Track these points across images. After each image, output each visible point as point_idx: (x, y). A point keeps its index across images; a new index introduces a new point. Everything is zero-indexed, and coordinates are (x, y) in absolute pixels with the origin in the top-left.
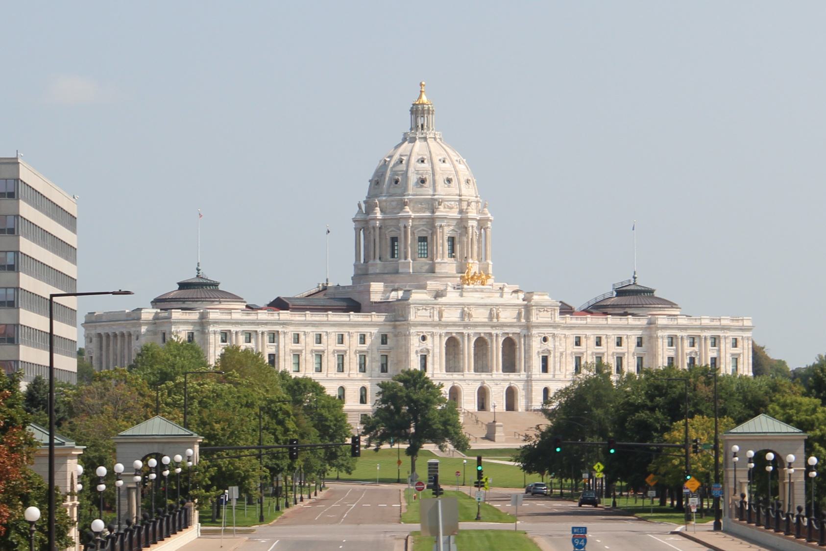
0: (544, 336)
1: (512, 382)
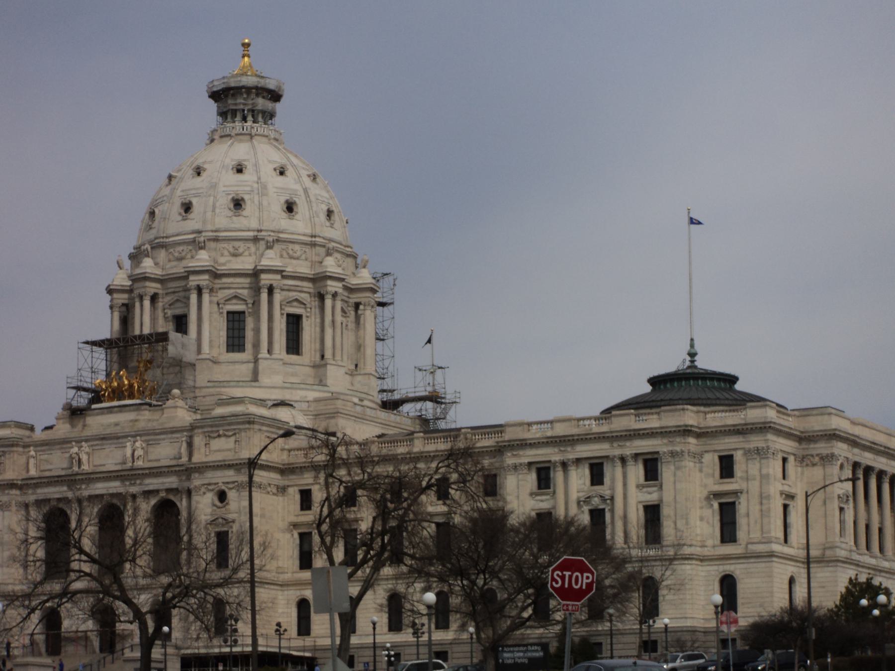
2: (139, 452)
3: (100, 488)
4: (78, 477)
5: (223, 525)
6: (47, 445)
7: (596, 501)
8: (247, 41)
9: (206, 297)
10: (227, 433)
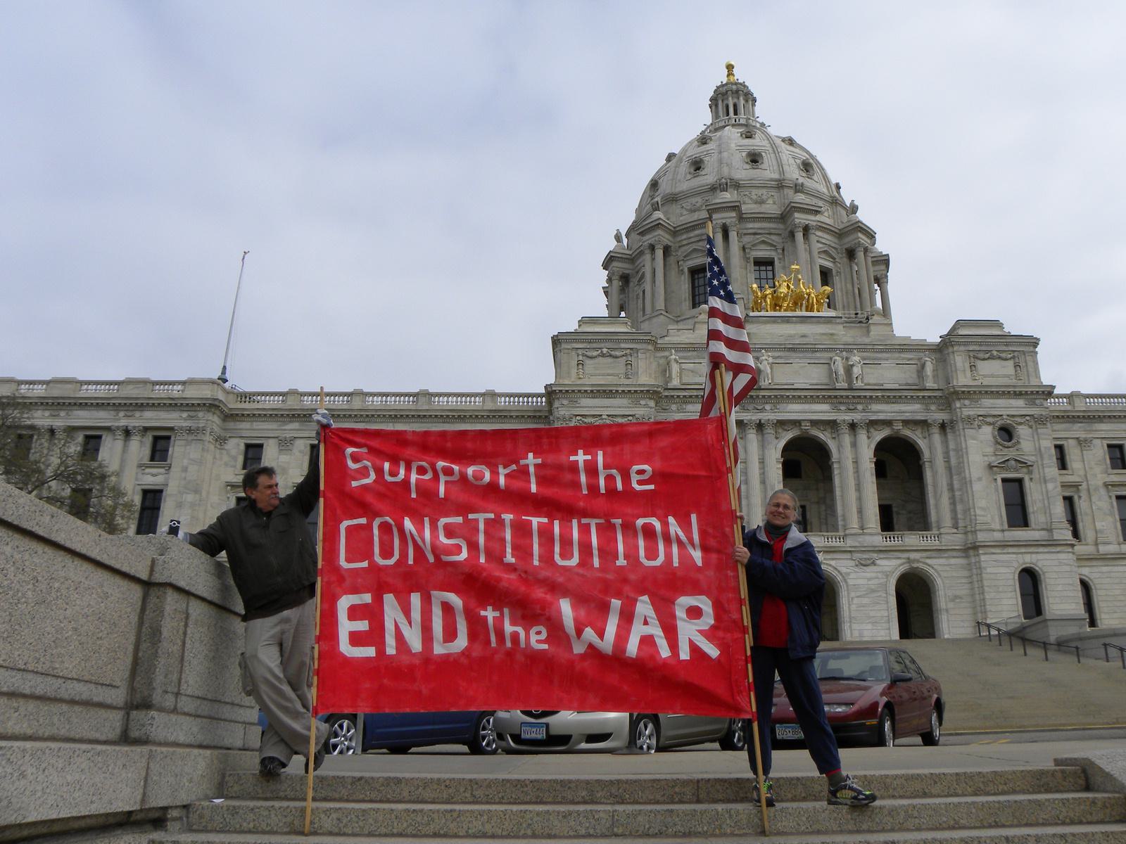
0: (999, 423)
1: (913, 556)
2: (856, 371)
3: (794, 411)
5: (1016, 470)
8: (733, 63)
9: (813, 238)
10: (1003, 355)
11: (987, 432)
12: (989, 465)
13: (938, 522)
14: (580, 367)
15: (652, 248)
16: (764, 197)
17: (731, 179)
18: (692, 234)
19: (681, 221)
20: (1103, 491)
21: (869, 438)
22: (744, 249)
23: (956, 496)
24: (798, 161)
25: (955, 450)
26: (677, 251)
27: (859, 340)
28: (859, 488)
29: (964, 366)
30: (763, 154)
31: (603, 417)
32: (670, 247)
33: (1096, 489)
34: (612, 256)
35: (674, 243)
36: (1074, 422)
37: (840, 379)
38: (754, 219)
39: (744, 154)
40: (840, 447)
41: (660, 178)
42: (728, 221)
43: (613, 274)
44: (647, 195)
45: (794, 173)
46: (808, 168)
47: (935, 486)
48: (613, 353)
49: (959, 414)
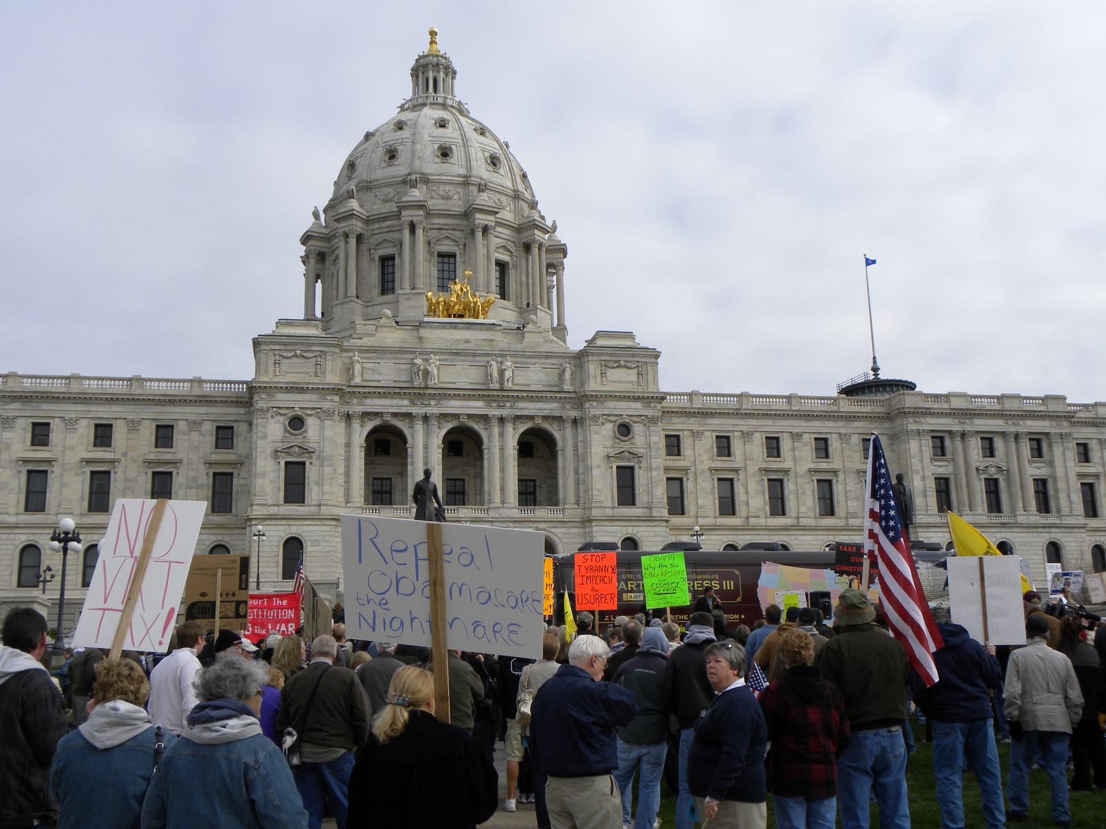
2: (508, 374)
3: (454, 406)
4: (428, 391)
5: (629, 460)
6: (374, 351)
7: (992, 470)
8: (436, 30)
9: (491, 237)
10: (629, 365)
11: (609, 429)
12: (608, 455)
13: (564, 498)
14: (277, 365)
15: (346, 235)
16: (451, 194)
17: (421, 174)
18: (384, 225)
19: (374, 210)
20: (707, 474)
21: (514, 429)
22: (429, 243)
23: (580, 479)
24: (487, 154)
25: (583, 442)
26: (369, 239)
27: (513, 347)
28: (503, 470)
29: (595, 373)
30: (454, 147)
31: (296, 409)
32: (363, 234)
33: (703, 472)
34: (309, 236)
35: (367, 231)
36: (690, 417)
37: (494, 380)
38: (440, 216)
39: (436, 146)
40: (490, 437)
41: (356, 159)
42: (415, 219)
43: (310, 252)
44: (345, 172)
45: (482, 171)
46: (495, 161)
47: (564, 470)
48: (305, 354)
49: (587, 413)
